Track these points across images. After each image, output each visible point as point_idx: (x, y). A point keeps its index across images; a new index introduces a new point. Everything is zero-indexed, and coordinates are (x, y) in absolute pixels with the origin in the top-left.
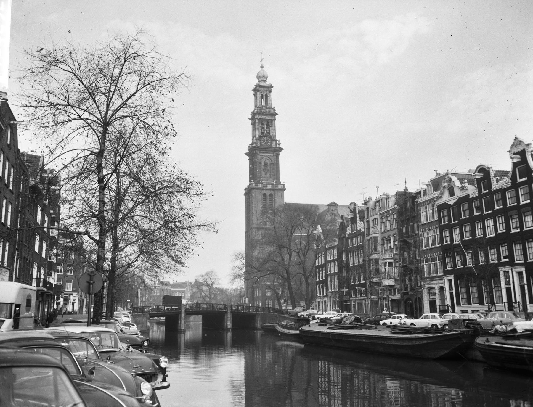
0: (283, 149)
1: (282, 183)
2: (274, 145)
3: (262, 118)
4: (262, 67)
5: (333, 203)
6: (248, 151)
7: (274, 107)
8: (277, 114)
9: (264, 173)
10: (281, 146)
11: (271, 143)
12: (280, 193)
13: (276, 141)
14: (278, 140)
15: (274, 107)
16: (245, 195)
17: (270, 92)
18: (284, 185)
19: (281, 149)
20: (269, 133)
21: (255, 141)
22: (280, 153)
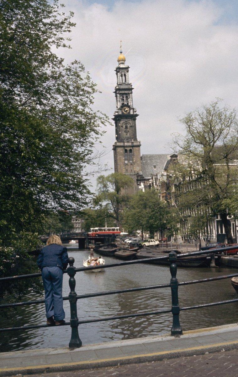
0: (138, 115)
1: (138, 140)
2: (132, 113)
3: (122, 92)
4: (121, 53)
5: (174, 155)
6: (114, 117)
7: (131, 83)
8: (133, 89)
9: (125, 134)
10: (137, 113)
11: (130, 111)
12: (137, 148)
13: (133, 109)
15: (131, 83)
16: (113, 149)
17: (128, 71)
18: (140, 142)
19: (137, 115)
20: (128, 104)
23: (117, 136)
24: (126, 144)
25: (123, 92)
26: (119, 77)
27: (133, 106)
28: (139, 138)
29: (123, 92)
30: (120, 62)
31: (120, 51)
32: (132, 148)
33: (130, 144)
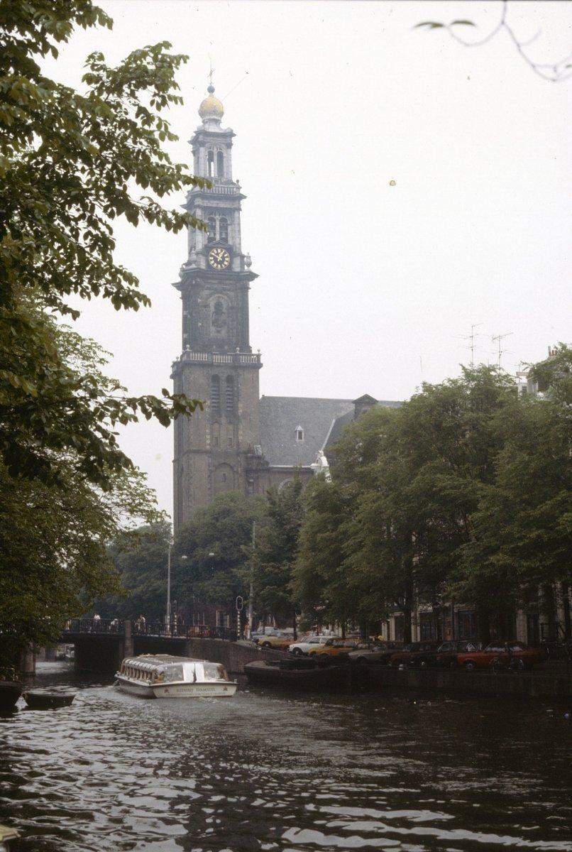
0: (256, 276)
1: (254, 351)
2: (237, 268)
3: (209, 205)
4: (211, 90)
6: (179, 280)
7: (238, 181)
8: (245, 197)
10: (253, 269)
11: (231, 263)
12: (248, 375)
13: (243, 257)
14: (246, 254)
15: (238, 181)
16: (172, 377)
17: (229, 146)
18: (258, 356)
20: (226, 240)
21: (194, 257)
22: (251, 284)
23: (185, 336)
24: (218, 359)
25: (213, 204)
26: (202, 161)
27: (240, 249)
28: (256, 341)
29: (213, 204)
30: (208, 117)
31: (209, 85)
32: (233, 373)
33: (228, 359)
